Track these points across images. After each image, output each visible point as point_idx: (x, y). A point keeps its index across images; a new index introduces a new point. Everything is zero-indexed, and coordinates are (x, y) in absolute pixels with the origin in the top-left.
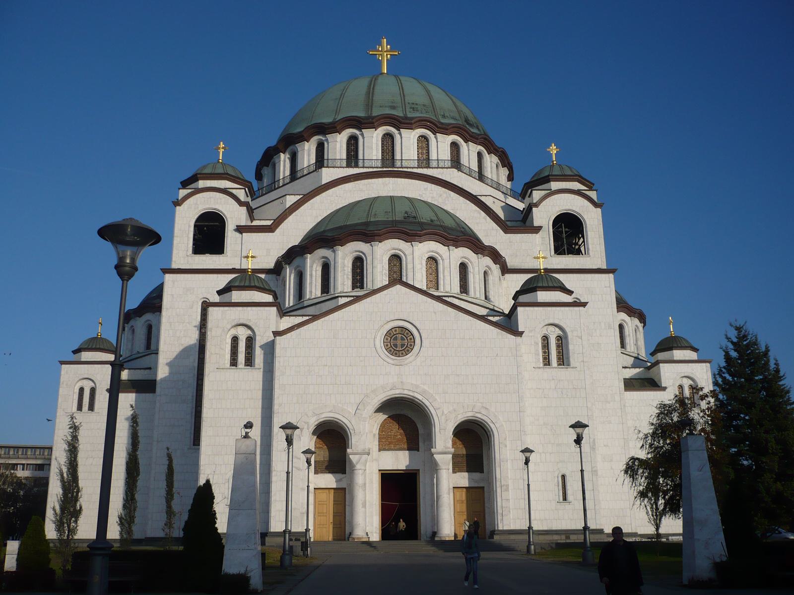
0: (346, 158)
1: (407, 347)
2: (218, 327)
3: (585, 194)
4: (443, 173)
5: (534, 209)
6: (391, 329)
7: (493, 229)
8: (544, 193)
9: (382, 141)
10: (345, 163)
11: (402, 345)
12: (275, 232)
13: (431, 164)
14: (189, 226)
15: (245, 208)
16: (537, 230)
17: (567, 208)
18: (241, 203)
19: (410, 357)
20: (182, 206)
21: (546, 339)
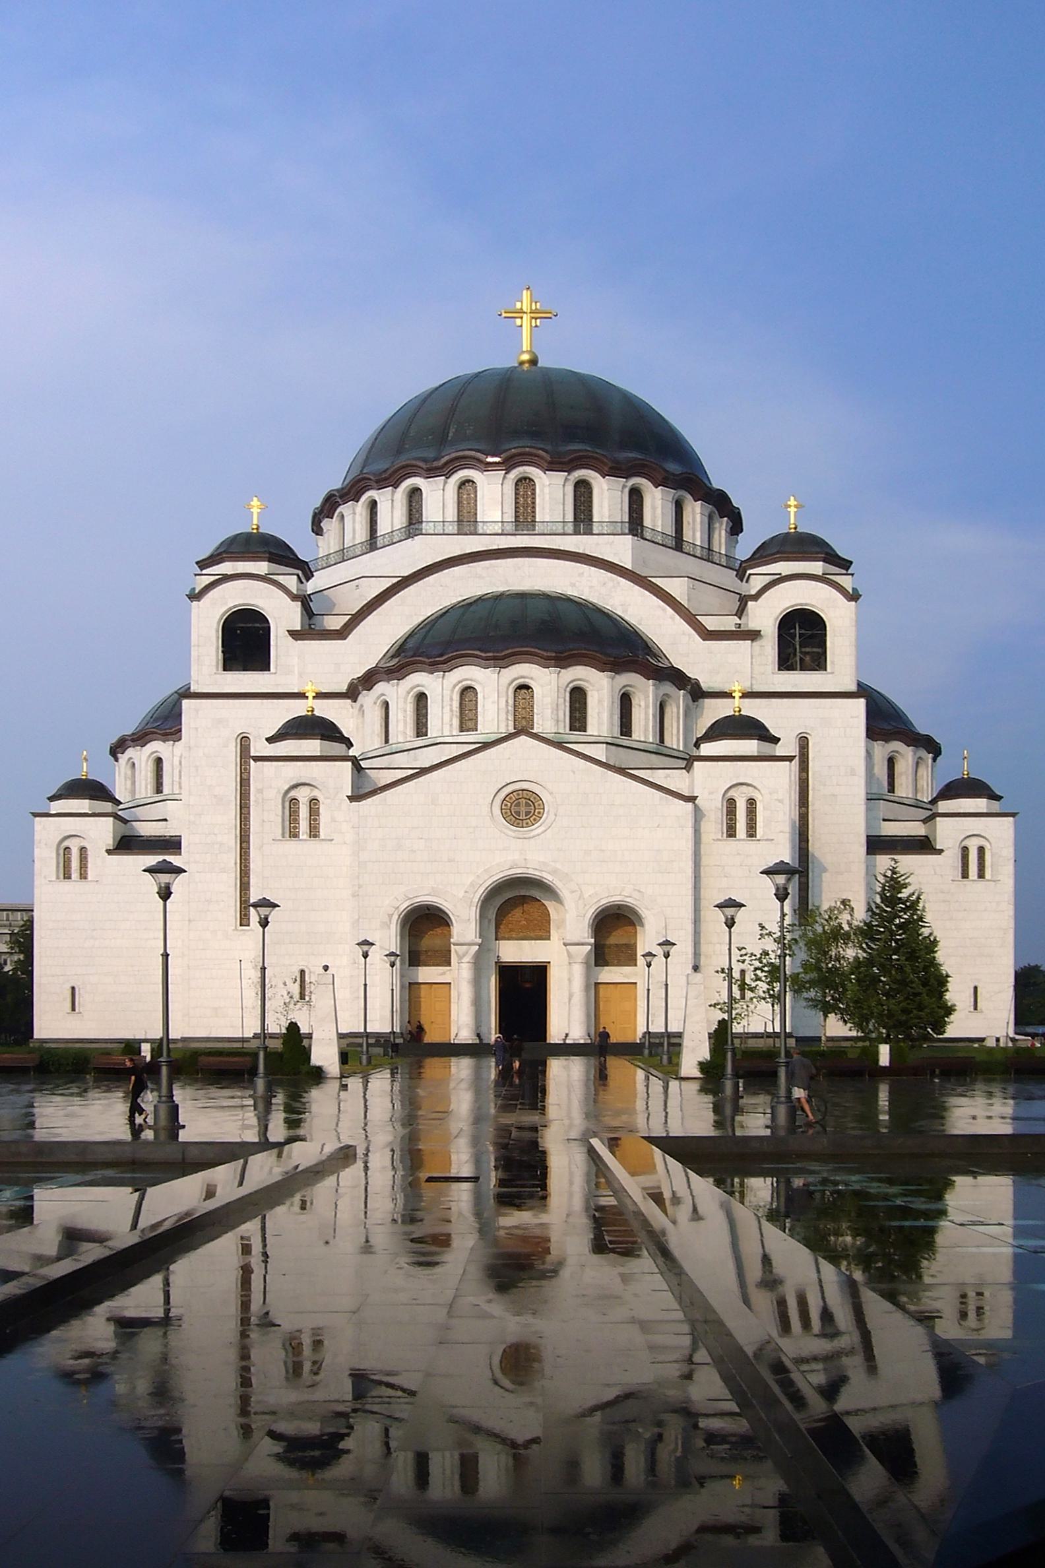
0: (456, 519)
1: (534, 814)
2: (271, 787)
3: (831, 580)
4: (613, 542)
5: (750, 603)
6: (512, 793)
7: (684, 634)
8: (769, 579)
9: (516, 489)
10: (456, 528)
11: (527, 813)
12: (348, 639)
13: (594, 528)
14: (218, 631)
15: (300, 603)
16: (753, 635)
17: (803, 602)
18: (294, 598)
19: (537, 829)
20: (202, 601)
21: (731, 805)
